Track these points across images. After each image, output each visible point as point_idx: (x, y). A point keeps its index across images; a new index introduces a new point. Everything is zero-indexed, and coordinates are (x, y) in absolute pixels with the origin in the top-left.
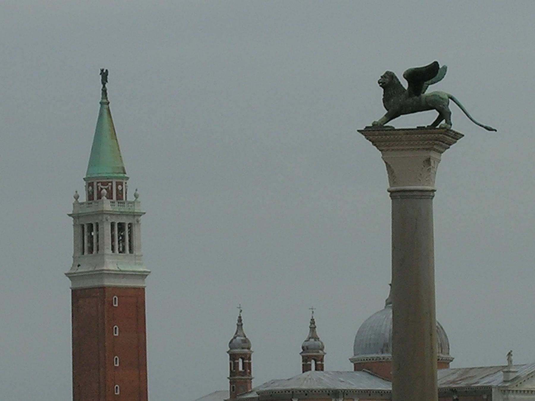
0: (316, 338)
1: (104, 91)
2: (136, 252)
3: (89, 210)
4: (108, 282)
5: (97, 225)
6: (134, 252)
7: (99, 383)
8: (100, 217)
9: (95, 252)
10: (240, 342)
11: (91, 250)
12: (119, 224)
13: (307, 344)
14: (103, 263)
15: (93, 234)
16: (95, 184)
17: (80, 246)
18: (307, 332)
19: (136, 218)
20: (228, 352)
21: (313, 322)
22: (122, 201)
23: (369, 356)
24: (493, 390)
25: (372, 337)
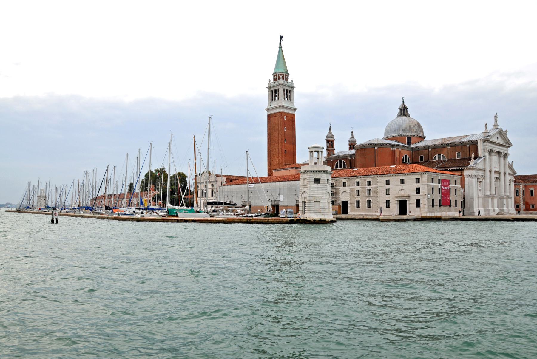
0: (354, 138)
1: (280, 43)
2: (292, 100)
5: (278, 89)
7: (279, 149)
8: (280, 86)
11: (275, 100)
13: (351, 139)
14: (282, 103)
16: (277, 75)
17: (271, 98)
18: (350, 136)
21: (352, 132)
23: (397, 134)
24: (479, 141)
25: (397, 127)
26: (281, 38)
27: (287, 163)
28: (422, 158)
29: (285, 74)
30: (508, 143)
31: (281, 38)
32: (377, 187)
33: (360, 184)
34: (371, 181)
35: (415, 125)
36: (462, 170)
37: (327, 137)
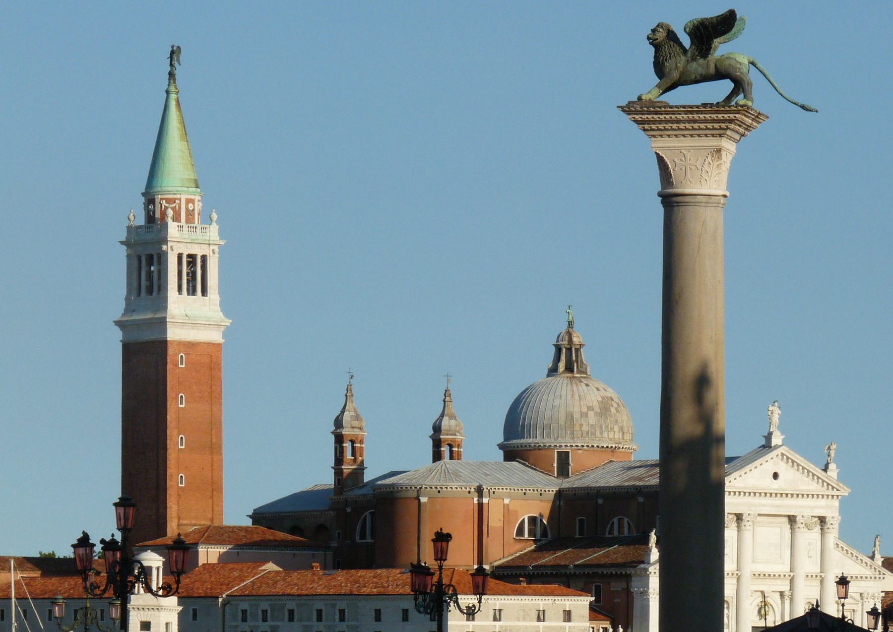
1: (171, 75)
3: (149, 237)
4: (173, 334)
6: (208, 295)
9: (155, 293)
10: (349, 419)
11: (150, 291)
12: (189, 256)
14: (165, 308)
15: (152, 268)
16: (157, 201)
17: (135, 284)
19: (212, 247)
20: (332, 433)
21: (447, 393)
22: (192, 225)
26: (174, 53)
27: (185, 522)
28: (581, 521)
29: (183, 198)
30: (828, 484)
31: (174, 53)
32: (358, 627)
33: (324, 617)
34: (347, 611)
35: (590, 408)
36: (628, 577)
37: (338, 423)
